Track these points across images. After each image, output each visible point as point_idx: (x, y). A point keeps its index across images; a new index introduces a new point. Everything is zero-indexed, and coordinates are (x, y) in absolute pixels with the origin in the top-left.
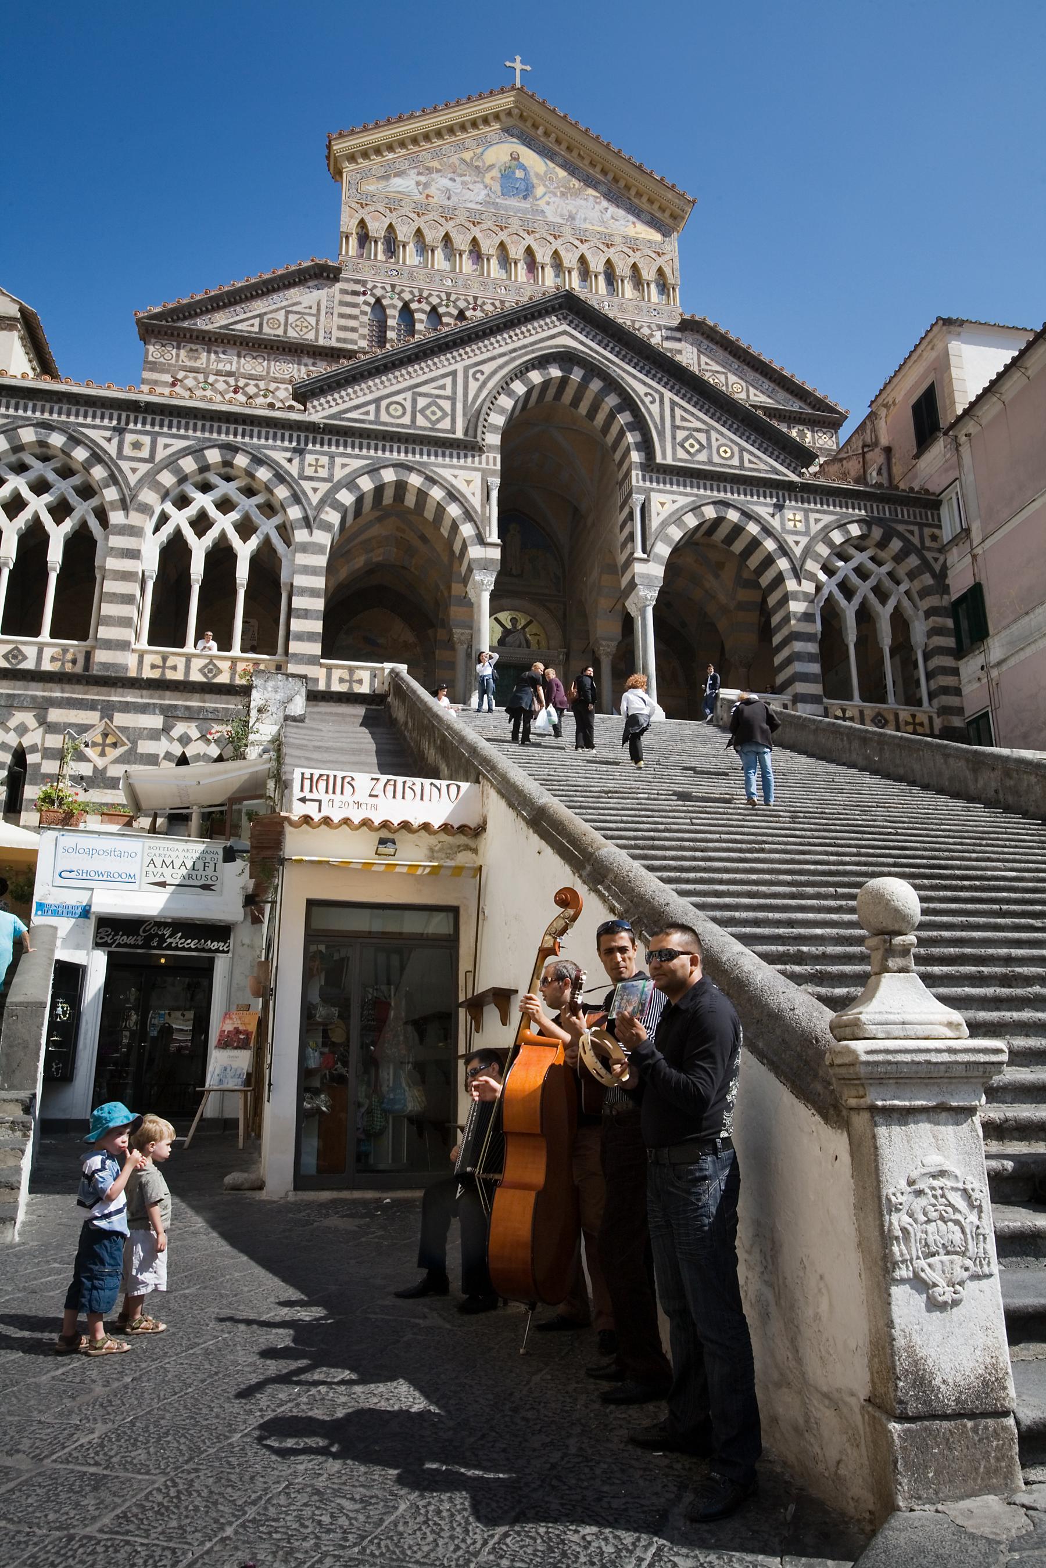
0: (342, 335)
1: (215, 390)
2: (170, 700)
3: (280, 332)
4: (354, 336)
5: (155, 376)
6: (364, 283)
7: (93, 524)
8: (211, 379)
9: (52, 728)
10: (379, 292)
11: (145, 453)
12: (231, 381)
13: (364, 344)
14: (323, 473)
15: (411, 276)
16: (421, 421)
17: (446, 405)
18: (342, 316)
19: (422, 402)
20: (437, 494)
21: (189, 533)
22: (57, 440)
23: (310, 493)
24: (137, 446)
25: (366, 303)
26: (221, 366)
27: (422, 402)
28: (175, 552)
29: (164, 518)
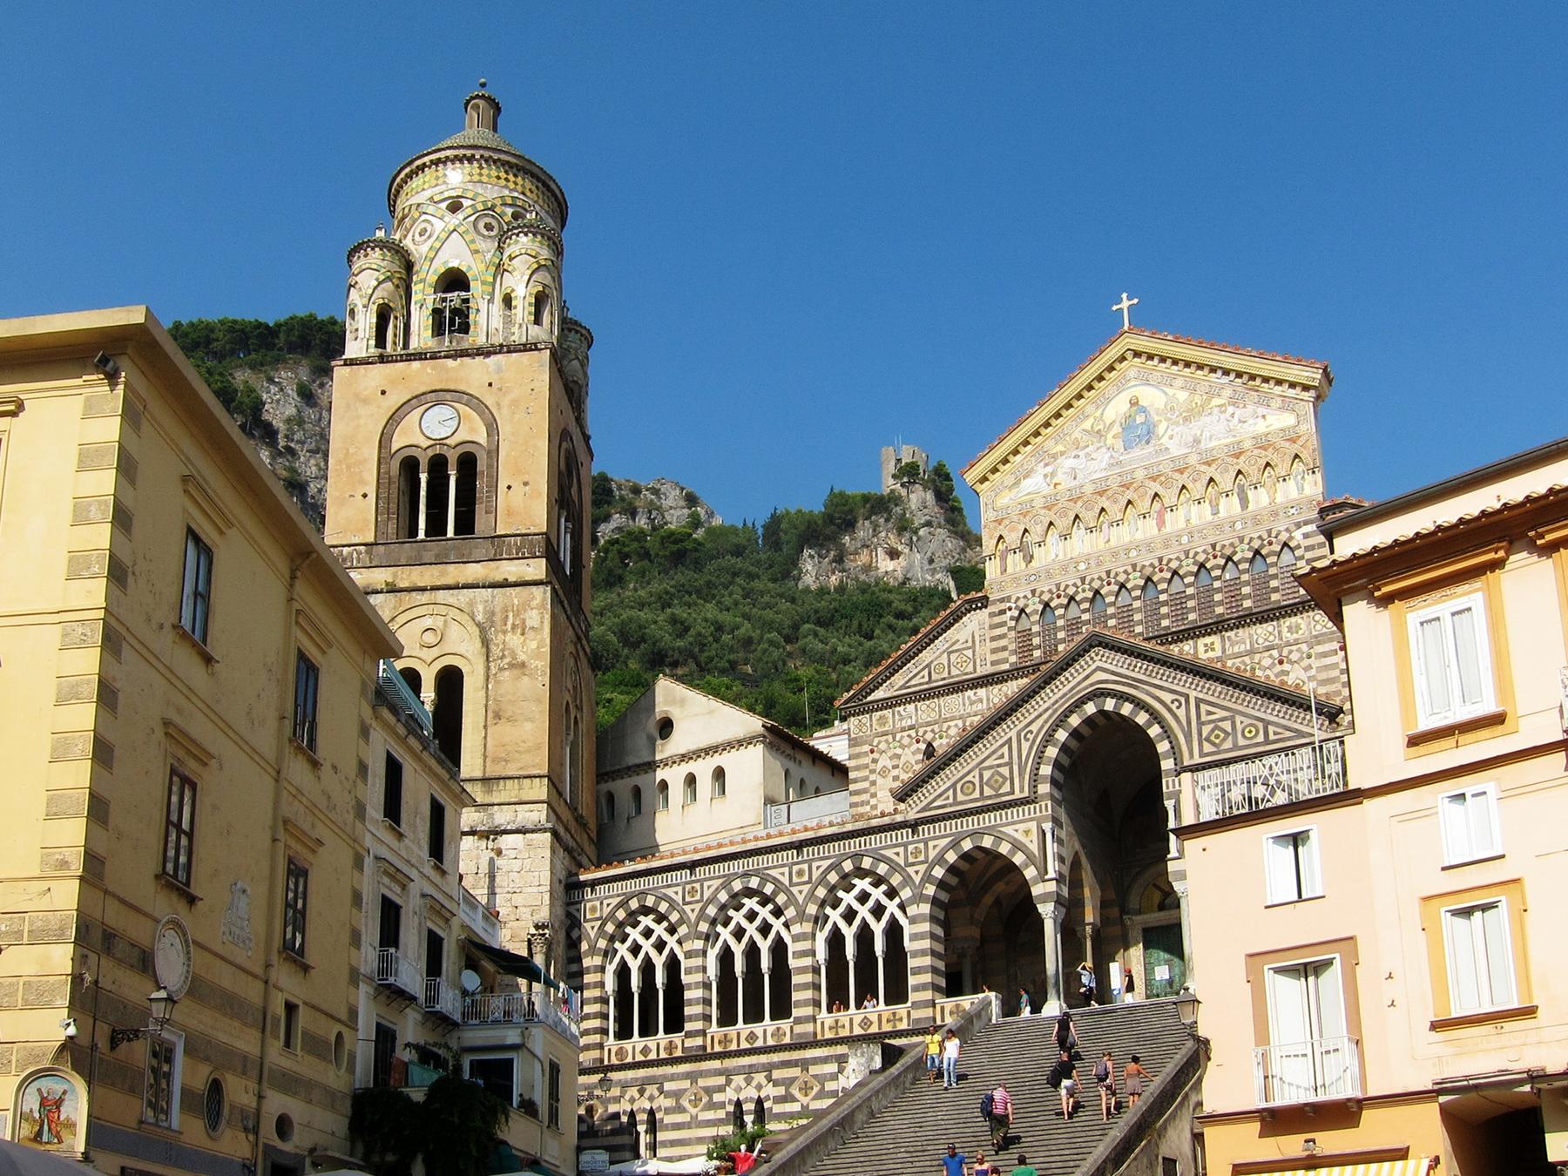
0: (995, 657)
1: (903, 747)
2: (841, 1049)
3: (945, 674)
4: (1005, 654)
5: (857, 750)
6: (1008, 599)
7: (784, 933)
8: (898, 736)
9: (776, 1083)
10: (1021, 604)
11: (806, 878)
12: (912, 733)
13: (1013, 659)
14: (922, 858)
15: (1049, 575)
16: (988, 791)
17: (1005, 771)
18: (993, 639)
19: (987, 775)
20: (1004, 849)
21: (842, 925)
22: (754, 883)
23: (913, 875)
24: (800, 873)
25: (1012, 618)
26: (904, 724)
27: (987, 775)
28: (836, 940)
29: (827, 918)
